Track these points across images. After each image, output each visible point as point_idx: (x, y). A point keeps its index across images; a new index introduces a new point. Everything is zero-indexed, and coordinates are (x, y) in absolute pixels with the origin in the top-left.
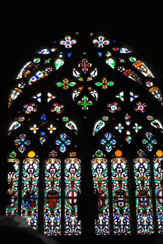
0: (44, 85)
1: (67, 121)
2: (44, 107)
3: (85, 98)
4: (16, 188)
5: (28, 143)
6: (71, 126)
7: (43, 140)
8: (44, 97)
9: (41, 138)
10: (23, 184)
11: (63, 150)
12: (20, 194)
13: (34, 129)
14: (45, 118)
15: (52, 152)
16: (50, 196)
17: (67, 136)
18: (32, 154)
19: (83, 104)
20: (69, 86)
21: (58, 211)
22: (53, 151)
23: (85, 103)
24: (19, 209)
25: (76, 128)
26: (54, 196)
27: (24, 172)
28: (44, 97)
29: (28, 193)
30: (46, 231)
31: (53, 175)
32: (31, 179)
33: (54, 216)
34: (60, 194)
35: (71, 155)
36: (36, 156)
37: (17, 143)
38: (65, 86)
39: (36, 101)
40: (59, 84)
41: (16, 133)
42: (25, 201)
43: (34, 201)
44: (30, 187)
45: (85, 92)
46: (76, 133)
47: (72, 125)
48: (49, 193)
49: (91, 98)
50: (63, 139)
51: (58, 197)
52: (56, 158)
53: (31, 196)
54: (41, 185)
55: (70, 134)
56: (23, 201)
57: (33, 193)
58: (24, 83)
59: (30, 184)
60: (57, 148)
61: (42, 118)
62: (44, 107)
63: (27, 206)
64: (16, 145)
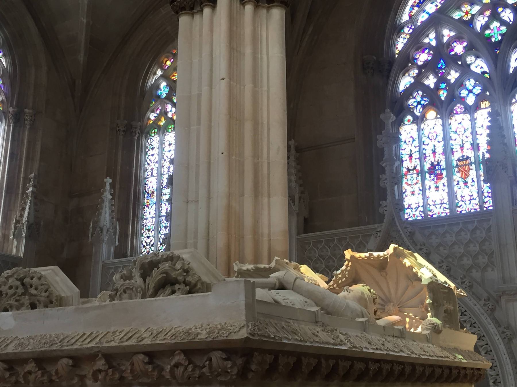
0: (436, 21)
1: (473, 62)
2: (441, 52)
3: (495, 24)
4: (418, 160)
5: (426, 101)
6: (480, 67)
7: (443, 95)
8: (439, 37)
9: (441, 92)
10: (425, 154)
11: (471, 100)
12: (422, 166)
13: (431, 81)
14: (444, 64)
15: (457, 108)
16: (461, 163)
17: (476, 81)
18: (431, 114)
19: (493, 34)
20: (472, 15)
21: (473, 181)
22: (458, 105)
23: (496, 31)
24: (423, 184)
25: (486, 69)
26: (466, 162)
27: (424, 139)
28: (439, 37)
29: (432, 164)
30: (460, 207)
31: (461, 136)
32: (435, 146)
33: (468, 187)
34: (473, 160)
35: (483, 105)
36: (436, 117)
37: (412, 105)
38: (466, 16)
39: (429, 45)
40: (457, 15)
41: (409, 92)
42: (430, 175)
43: (441, 172)
44: (435, 157)
45: (495, 16)
46: (487, 76)
47: (479, 65)
48: (459, 160)
49: (503, 23)
50: (470, 88)
51: (471, 164)
52: (464, 112)
53: (437, 167)
54: (448, 151)
55: (479, 78)
56: (427, 175)
57: (438, 164)
58: (412, 26)
59: (434, 152)
60: (462, 100)
61: (439, 66)
62: (441, 52)
63: (433, 180)
64: (412, 107)
